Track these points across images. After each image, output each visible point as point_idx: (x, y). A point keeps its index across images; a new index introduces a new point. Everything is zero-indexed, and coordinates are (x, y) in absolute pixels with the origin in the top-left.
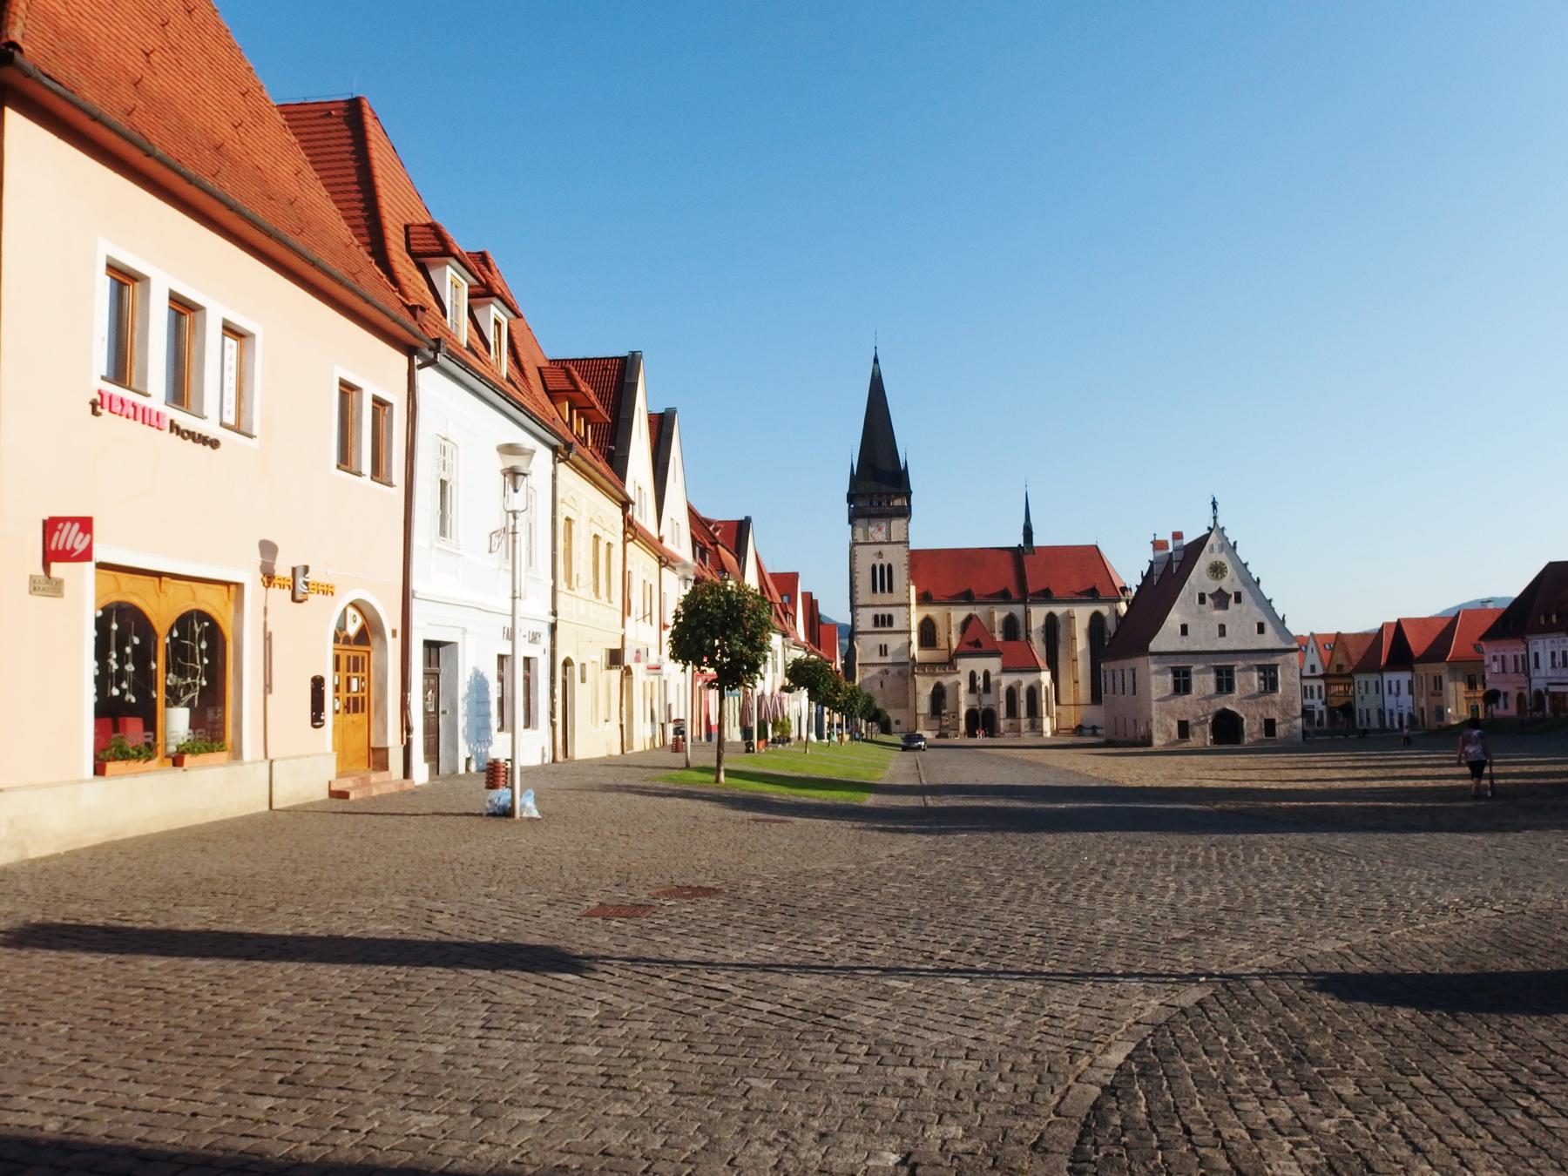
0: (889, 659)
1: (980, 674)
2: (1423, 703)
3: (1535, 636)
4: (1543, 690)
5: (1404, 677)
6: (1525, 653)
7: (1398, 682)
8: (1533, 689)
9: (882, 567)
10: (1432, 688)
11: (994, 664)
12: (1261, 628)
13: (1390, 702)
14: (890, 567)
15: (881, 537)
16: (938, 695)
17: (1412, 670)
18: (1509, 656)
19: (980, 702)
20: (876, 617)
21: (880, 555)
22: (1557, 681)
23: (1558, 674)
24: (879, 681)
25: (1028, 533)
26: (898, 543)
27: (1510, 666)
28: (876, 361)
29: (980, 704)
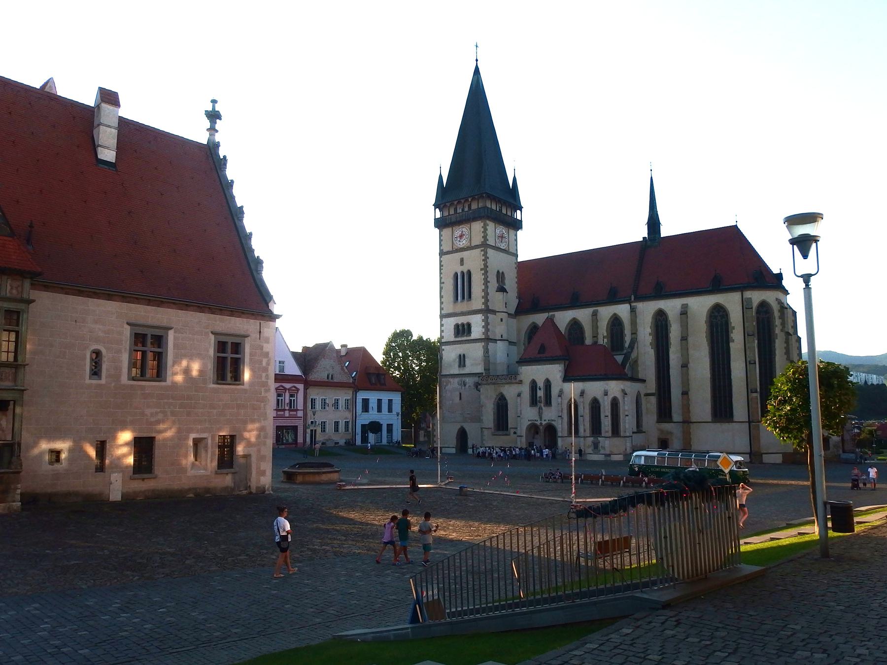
0: (467, 370)
1: (541, 384)
9: (463, 273)
11: (554, 372)
14: (469, 273)
15: (463, 243)
16: (502, 406)
19: (540, 415)
20: (457, 326)
21: (462, 260)
24: (458, 393)
25: (654, 223)
26: (477, 247)
28: (477, 71)
29: (541, 420)
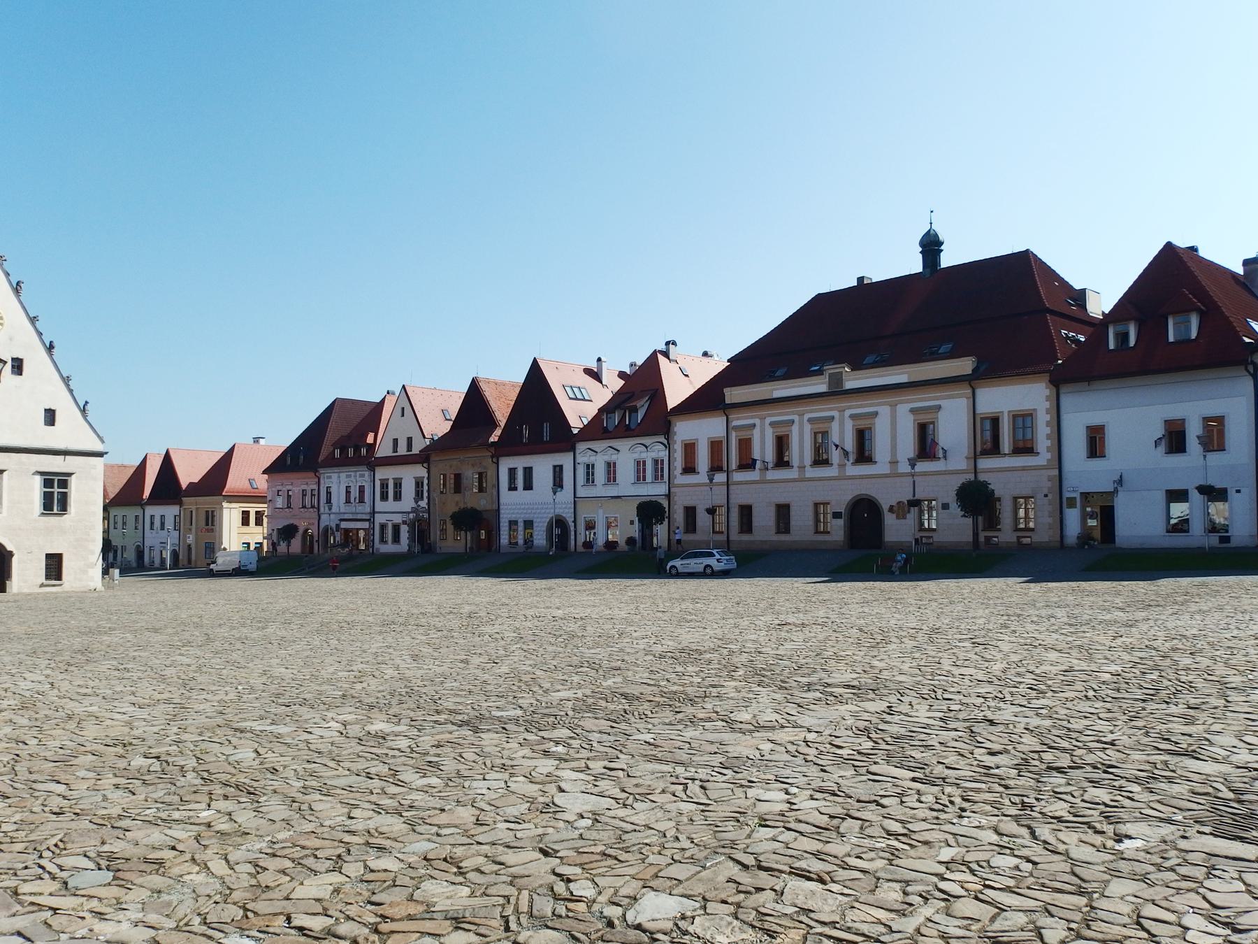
2: (191, 539)
3: (329, 470)
4: (334, 526)
5: (170, 511)
6: (315, 487)
7: (162, 517)
8: (322, 526)
10: (203, 522)
12: (50, 417)
13: (152, 539)
17: (181, 504)
18: (296, 490)
22: (351, 517)
23: (354, 510)
27: (296, 502)
